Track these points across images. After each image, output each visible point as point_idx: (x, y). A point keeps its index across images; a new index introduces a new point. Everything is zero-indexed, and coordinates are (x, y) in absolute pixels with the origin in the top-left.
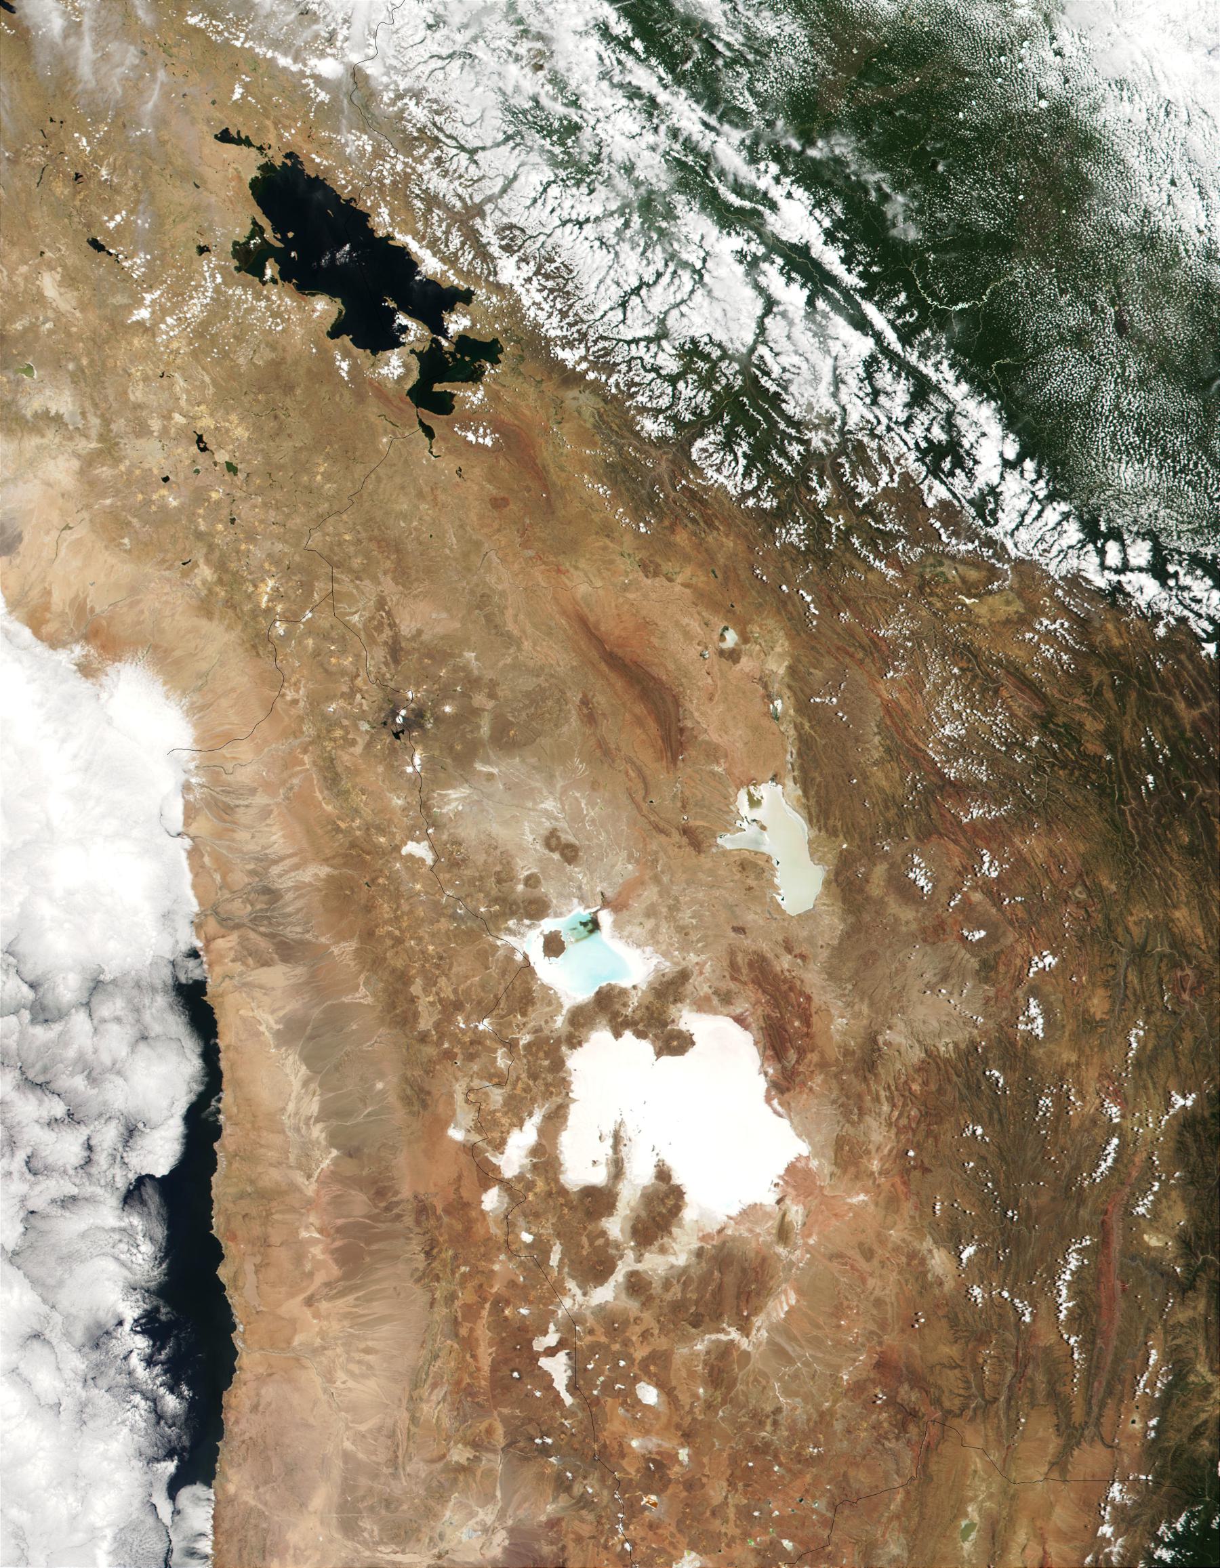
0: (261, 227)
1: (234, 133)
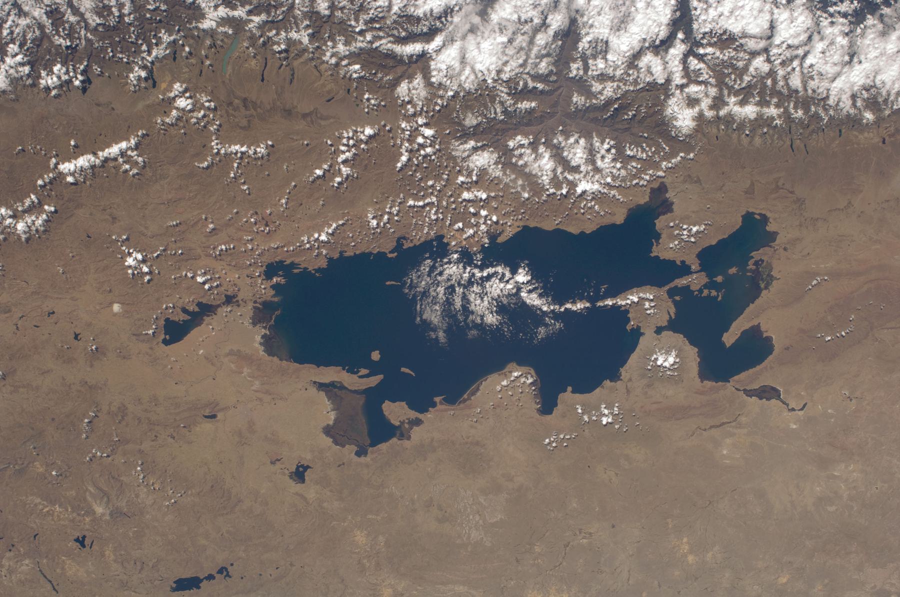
0: (332, 385)
1: (182, 317)
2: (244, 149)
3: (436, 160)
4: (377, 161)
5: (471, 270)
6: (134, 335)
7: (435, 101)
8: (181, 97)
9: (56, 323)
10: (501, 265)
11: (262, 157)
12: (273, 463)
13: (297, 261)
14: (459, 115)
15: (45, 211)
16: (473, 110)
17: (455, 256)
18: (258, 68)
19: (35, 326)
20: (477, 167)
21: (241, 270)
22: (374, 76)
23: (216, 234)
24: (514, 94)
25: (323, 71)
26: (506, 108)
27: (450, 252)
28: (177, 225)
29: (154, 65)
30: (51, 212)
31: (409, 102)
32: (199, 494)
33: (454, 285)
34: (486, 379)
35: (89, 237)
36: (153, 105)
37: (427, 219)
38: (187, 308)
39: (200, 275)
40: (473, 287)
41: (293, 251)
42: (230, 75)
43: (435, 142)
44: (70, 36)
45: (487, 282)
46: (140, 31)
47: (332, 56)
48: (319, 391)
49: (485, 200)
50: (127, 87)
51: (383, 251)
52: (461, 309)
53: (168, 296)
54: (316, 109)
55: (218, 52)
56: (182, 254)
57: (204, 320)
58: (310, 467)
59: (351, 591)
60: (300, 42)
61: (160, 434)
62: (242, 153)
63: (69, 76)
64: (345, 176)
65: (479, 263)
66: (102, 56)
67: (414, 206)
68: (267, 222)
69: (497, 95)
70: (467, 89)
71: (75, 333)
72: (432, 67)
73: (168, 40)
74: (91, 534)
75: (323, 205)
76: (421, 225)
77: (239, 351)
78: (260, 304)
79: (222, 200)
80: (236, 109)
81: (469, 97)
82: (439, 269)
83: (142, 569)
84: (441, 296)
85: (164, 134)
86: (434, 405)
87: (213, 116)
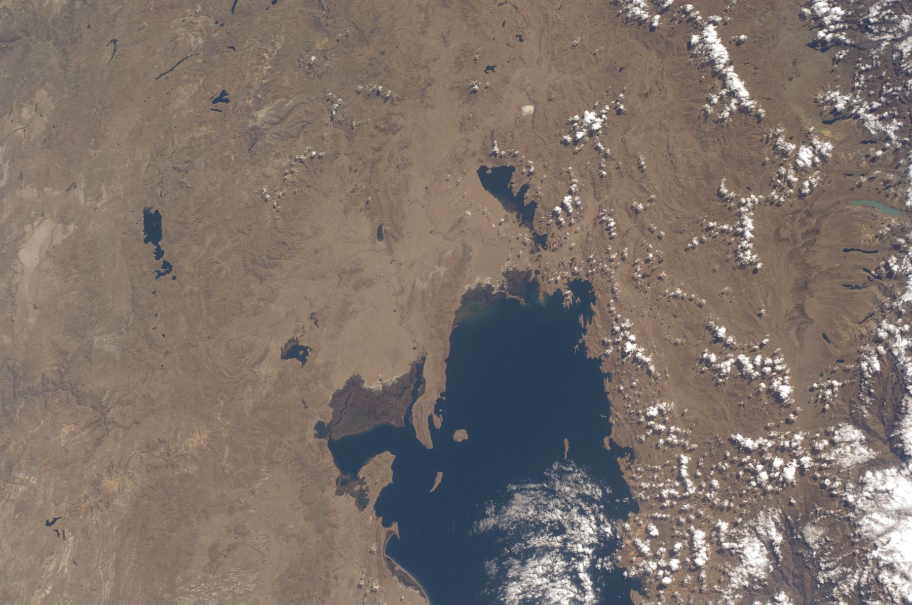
1: (516, 185)
2: (748, 234)
3: (749, 488)
4: (742, 407)
5: (588, 555)
6: (493, 132)
7: (838, 479)
8: (814, 153)
9: (507, 44)
10: (596, 599)
11: (739, 259)
12: (313, 316)
13: (596, 319)
14: (820, 515)
15: (652, 17)
16: (829, 535)
17: (608, 530)
18: (862, 242)
19: (504, 22)
20: (742, 549)
21: (581, 250)
22: (867, 393)
23: (629, 216)
24: (860, 596)
25: (867, 325)
26: (836, 585)
27: (614, 523)
28: (641, 167)
29: (854, 119)
30: (651, 23)
31: (833, 444)
32: (274, 228)
33: (565, 533)
34: (423, 596)
35: (621, 69)
36: (800, 124)
37: (661, 485)
38: (529, 191)
39: (573, 199)
40: (562, 560)
41: (610, 312)
42: (848, 209)
43: (777, 484)
44: (882, 22)
45: (571, 580)
46: (898, 98)
47: (888, 332)
48: (412, 365)
49: (695, 564)
50: (822, 92)
51: (613, 430)
52: (528, 547)
53: (544, 166)
54: (812, 322)
55: (880, 192)
56: (602, 176)
57: (512, 212)
58: (303, 364)
59: (121, 435)
60: (904, 292)
61: (359, 175)
62: (742, 234)
63: (829, 25)
64: (718, 366)
65: (599, 566)
66: (860, 59)
67: (680, 465)
68: (649, 276)
69: (855, 568)
70: (860, 523)
71: (495, 66)
72: (888, 471)
73: (889, 132)
74: (231, 108)
75: (676, 344)
76: (653, 477)
77: (470, 259)
78: (534, 279)
79: (677, 218)
80: (803, 222)
81: (847, 528)
82: (588, 509)
83: (179, 170)
84: (549, 515)
85: (761, 140)
86: (386, 524)
87: (790, 193)
